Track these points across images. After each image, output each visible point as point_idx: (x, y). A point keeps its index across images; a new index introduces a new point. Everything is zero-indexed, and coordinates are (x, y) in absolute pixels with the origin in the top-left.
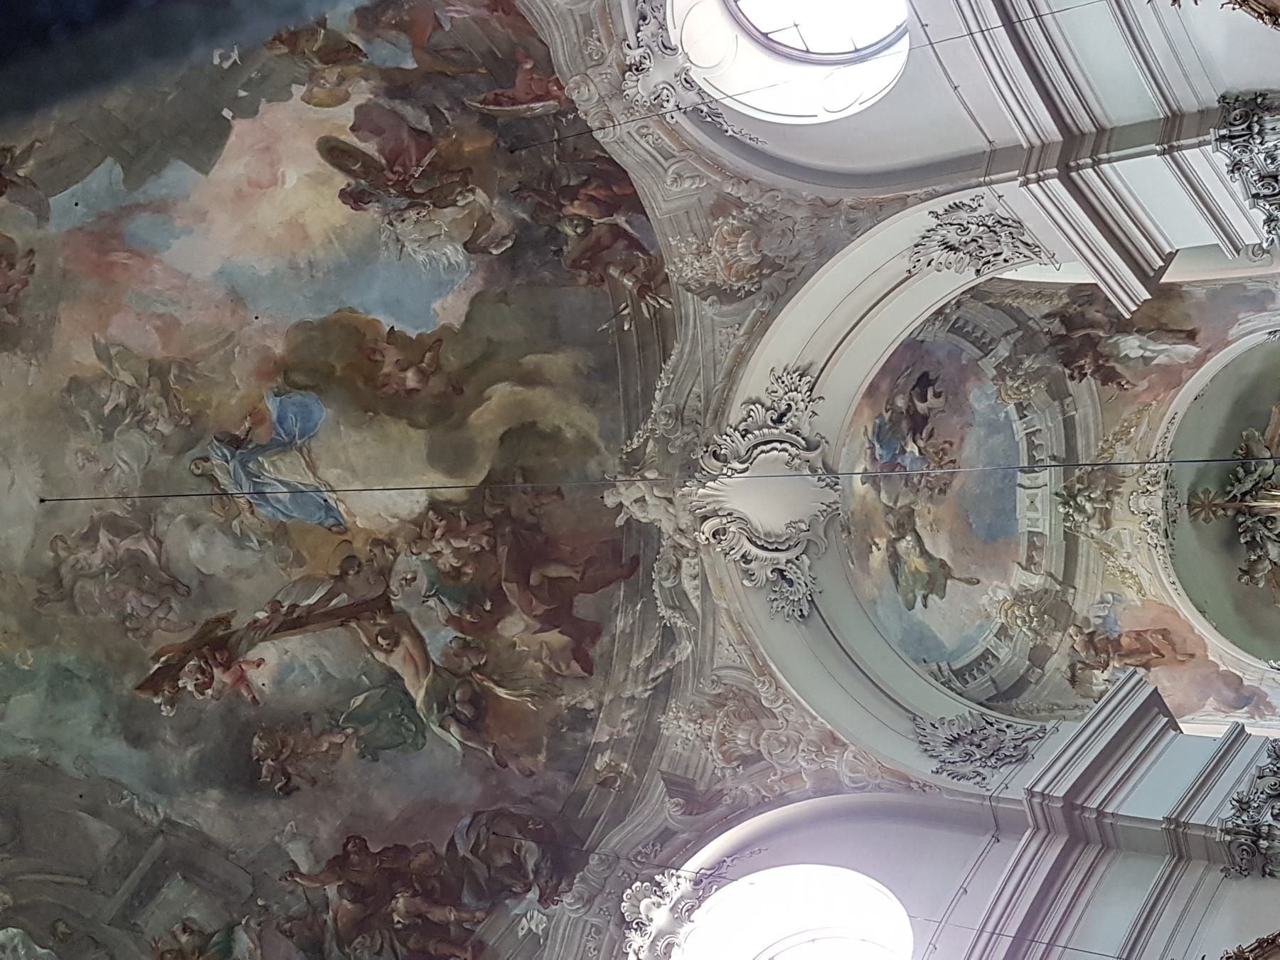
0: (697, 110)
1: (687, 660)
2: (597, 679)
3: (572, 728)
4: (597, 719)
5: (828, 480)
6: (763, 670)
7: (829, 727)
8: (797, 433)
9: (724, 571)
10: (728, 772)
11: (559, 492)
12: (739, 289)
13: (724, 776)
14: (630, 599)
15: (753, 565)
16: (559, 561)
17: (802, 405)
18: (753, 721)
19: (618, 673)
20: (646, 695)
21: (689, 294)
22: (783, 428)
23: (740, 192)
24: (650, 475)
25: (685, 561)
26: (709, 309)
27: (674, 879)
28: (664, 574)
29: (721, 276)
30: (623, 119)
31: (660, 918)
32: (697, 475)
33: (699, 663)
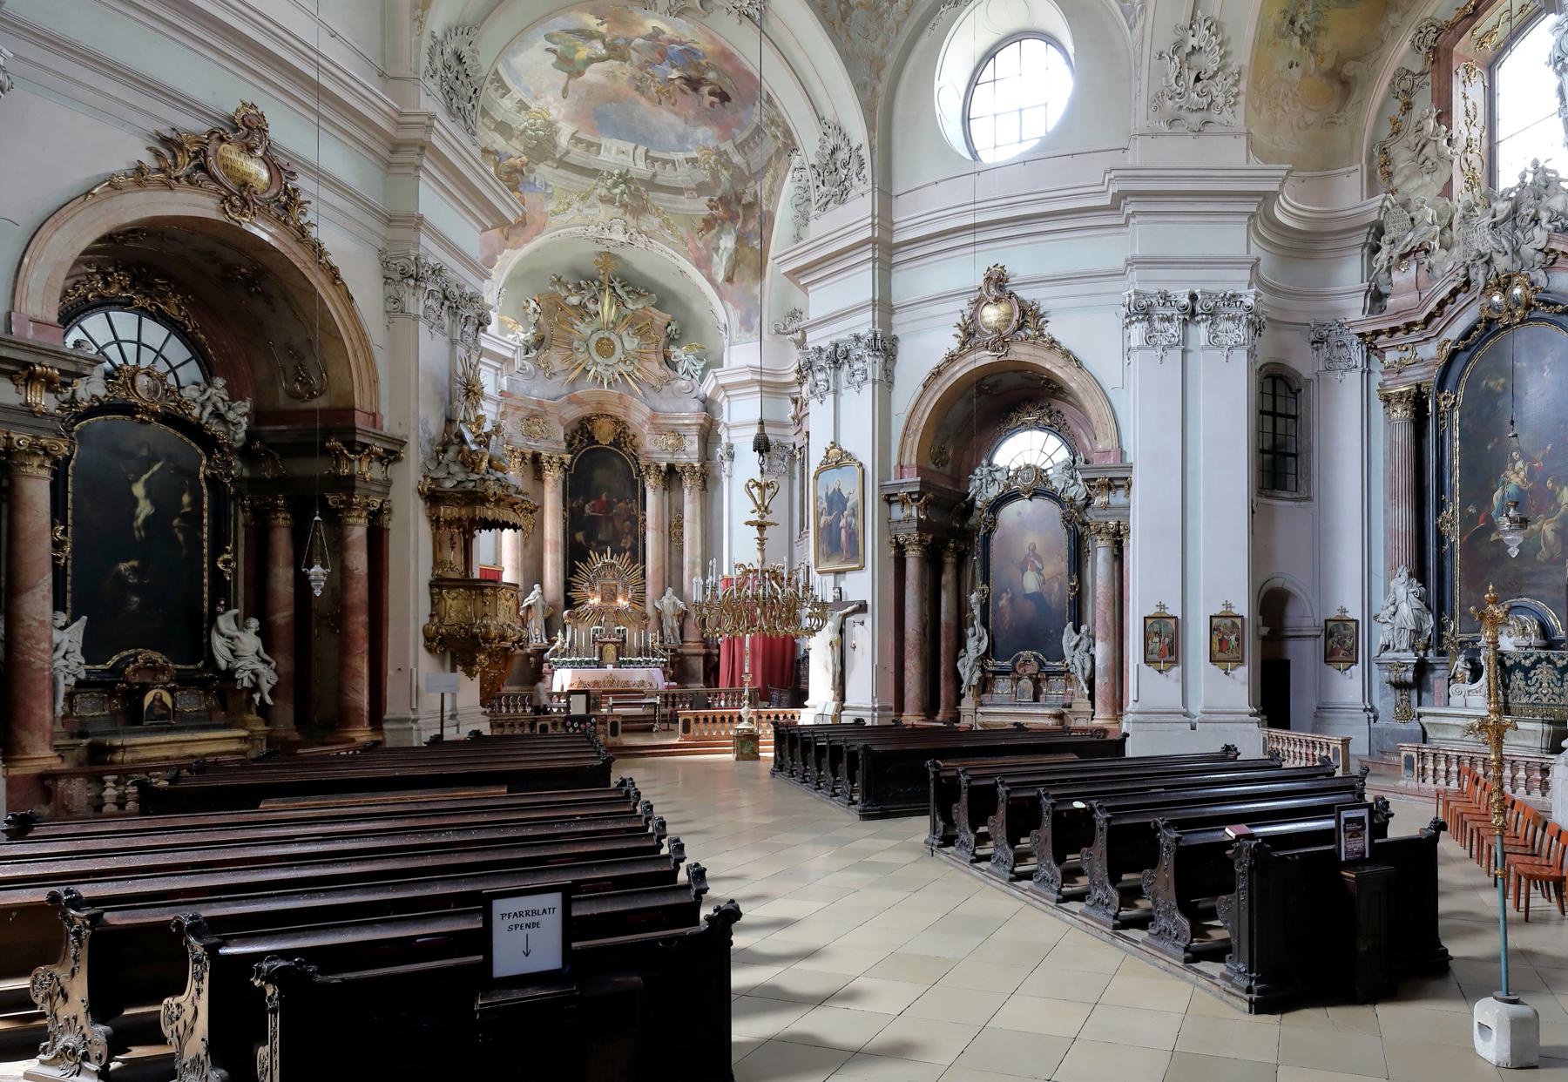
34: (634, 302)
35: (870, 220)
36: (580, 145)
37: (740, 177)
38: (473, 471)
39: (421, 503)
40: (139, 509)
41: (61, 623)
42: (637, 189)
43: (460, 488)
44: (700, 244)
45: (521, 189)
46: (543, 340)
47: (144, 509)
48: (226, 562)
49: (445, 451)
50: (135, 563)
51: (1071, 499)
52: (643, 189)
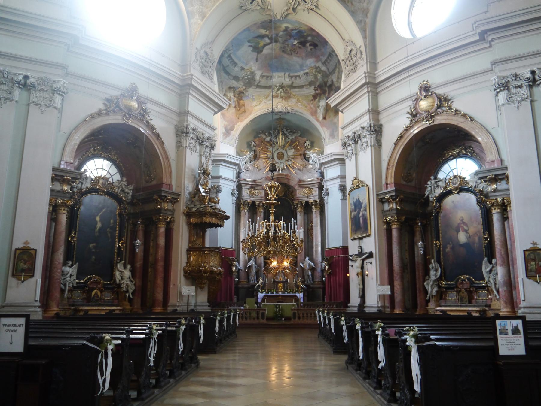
5: (284, 15)
7: (208, 15)
8: (298, 5)
17: (307, 6)
34: (292, 135)
35: (364, 75)
36: (264, 78)
37: (325, 75)
38: (203, 204)
39: (184, 217)
40: (97, 225)
41: (70, 265)
42: (286, 90)
43: (198, 211)
45: (243, 99)
46: (256, 157)
47: (99, 225)
48: (122, 244)
49: (194, 197)
50: (94, 244)
51: (480, 190)
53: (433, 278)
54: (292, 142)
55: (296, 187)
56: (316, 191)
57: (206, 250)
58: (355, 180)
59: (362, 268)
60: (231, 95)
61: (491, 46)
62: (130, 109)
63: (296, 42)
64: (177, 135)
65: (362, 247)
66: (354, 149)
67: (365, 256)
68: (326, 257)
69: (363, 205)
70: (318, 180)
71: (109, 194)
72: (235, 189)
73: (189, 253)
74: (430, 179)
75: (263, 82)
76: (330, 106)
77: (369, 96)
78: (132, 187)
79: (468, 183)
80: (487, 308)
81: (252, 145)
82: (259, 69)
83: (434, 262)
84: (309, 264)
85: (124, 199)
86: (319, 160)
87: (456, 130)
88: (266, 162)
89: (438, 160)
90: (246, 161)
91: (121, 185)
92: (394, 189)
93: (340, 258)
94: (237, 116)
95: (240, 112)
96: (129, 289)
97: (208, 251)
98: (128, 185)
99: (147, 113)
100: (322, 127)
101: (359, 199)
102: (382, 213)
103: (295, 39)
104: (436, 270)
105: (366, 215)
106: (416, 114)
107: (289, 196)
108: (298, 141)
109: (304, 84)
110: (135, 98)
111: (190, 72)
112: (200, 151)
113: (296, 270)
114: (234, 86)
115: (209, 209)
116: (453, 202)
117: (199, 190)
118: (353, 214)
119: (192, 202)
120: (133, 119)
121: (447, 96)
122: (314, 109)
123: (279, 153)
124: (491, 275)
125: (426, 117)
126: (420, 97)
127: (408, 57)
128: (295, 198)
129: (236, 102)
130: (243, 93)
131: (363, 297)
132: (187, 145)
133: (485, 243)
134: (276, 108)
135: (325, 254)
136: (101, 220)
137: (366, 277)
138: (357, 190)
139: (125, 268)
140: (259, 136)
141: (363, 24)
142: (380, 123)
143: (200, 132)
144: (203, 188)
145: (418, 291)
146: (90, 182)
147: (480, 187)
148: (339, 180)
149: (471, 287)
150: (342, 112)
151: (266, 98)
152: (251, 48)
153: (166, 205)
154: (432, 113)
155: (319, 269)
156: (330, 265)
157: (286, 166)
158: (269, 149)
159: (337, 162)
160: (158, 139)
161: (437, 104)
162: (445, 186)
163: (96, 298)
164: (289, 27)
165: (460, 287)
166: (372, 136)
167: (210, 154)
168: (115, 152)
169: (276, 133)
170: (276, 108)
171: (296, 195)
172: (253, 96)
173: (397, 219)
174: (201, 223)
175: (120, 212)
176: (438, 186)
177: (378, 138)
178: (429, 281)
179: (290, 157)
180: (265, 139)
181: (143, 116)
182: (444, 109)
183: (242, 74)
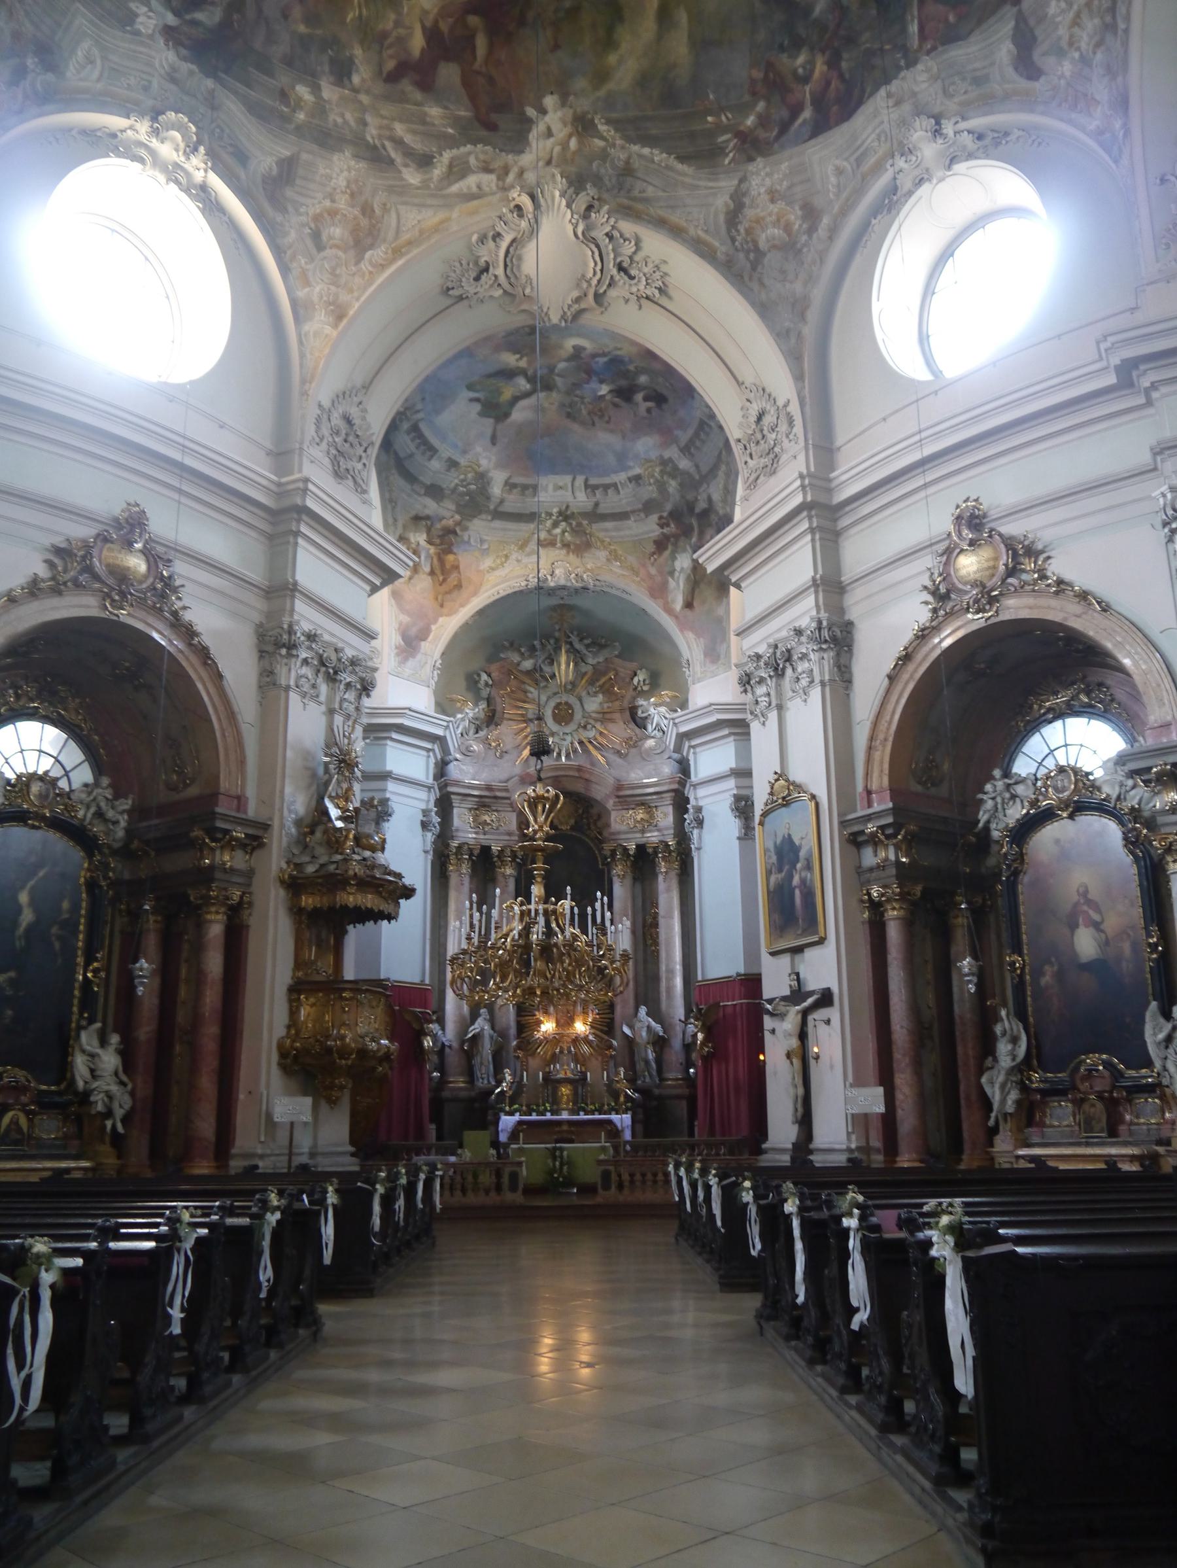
0: (895, 190)
1: (403, 179)
2: (379, 88)
3: (333, 62)
4: (343, 87)
6: (397, 252)
7: (351, 313)
8: (610, 285)
9: (484, 216)
10: (303, 219)
11: (556, 47)
12: (738, 231)
13: (300, 214)
14: (456, 121)
15: (491, 244)
16: (491, 46)
17: (634, 289)
18: (352, 243)
19: (387, 109)
20: (369, 139)
21: (736, 182)
22: (614, 271)
23: (822, 232)
24: (573, 144)
25: (493, 177)
26: (722, 202)
27: (203, 165)
28: (482, 157)
29: (749, 213)
30: (894, 116)
31: (166, 150)
32: (572, 190)
33: (401, 190)
34: (595, 655)
35: (798, 483)
36: (515, 491)
37: (691, 483)
38: (337, 852)
39: (282, 892)
42: (579, 525)
43: (322, 873)
44: (653, 571)
46: (494, 715)
47: (27, 917)
48: (96, 971)
49: (312, 832)
50: (12, 974)
51: (1133, 808)
52: (585, 522)
53: (1005, 1062)
54: (598, 673)
55: (610, 804)
56: (666, 815)
57: (345, 990)
58: (777, 780)
59: (803, 1036)
60: (420, 538)
61: (1149, 403)
62: (122, 576)
63: (604, 390)
64: (262, 654)
65: (801, 976)
66: (773, 693)
67: (810, 1001)
68: (697, 1005)
69: (802, 854)
70: (670, 783)
71: (58, 824)
72: (431, 811)
73: (295, 996)
74: (991, 778)
75: (513, 503)
76: (705, 569)
77: (813, 540)
78: (126, 804)
79: (1099, 789)
80: (1161, 1150)
81: (482, 682)
82: (500, 465)
83: (1008, 1015)
84: (649, 1027)
85: (103, 839)
86: (675, 724)
87: (1060, 639)
88: (522, 730)
89: (1013, 723)
90: (465, 728)
91: (94, 799)
92: (890, 805)
93: (738, 1008)
94: (436, 599)
95: (445, 587)
96: (116, 1105)
97: (351, 990)
98: (117, 796)
99: (175, 590)
100: (681, 631)
101: (789, 835)
102: (857, 876)
103: (601, 382)
104: (1015, 1040)
105: (811, 880)
106: (948, 592)
107: (589, 829)
108: (615, 669)
109: (629, 509)
110: (138, 546)
111: (300, 471)
112: (330, 700)
113: (610, 1047)
114: (427, 512)
115: (356, 868)
116: (1057, 841)
117: (326, 813)
118: (773, 879)
119: (306, 846)
120: (132, 605)
121: (1033, 542)
122: (658, 579)
123: (560, 704)
124: (1171, 1050)
125: (977, 601)
126: (956, 545)
127: (920, 432)
128: (605, 834)
129: (435, 560)
130: (455, 533)
131: (805, 1121)
132: (292, 683)
133: (1150, 960)
134: (549, 577)
135: (695, 995)
136: (33, 902)
137: (812, 1062)
138: (784, 809)
139: (103, 1043)
140: (502, 656)
141: (793, 341)
142: (847, 618)
143: (329, 644)
144: (337, 807)
145: (963, 1102)
146: (2, 790)
147: (1133, 799)
148: (731, 783)
149: (1114, 1087)
150: (738, 586)
151: (522, 547)
152: (477, 407)
153: (227, 858)
154: (992, 590)
155: (677, 1043)
156: (708, 1030)
157: (581, 743)
158: (529, 695)
159: (726, 732)
160: (205, 664)
161: (1006, 565)
162: (1033, 797)
163: (15, 1136)
164: (584, 349)
165: (1082, 1088)
166: (825, 656)
167: (357, 709)
168: (77, 701)
169: (549, 647)
170: (549, 577)
171: (608, 825)
172: (482, 541)
173: (900, 894)
174: (332, 909)
175: (91, 877)
176: (1014, 797)
177: (842, 661)
178: (995, 1072)
179: (590, 717)
180: (518, 664)
181: (163, 596)
182: (1024, 577)
183: (451, 480)
